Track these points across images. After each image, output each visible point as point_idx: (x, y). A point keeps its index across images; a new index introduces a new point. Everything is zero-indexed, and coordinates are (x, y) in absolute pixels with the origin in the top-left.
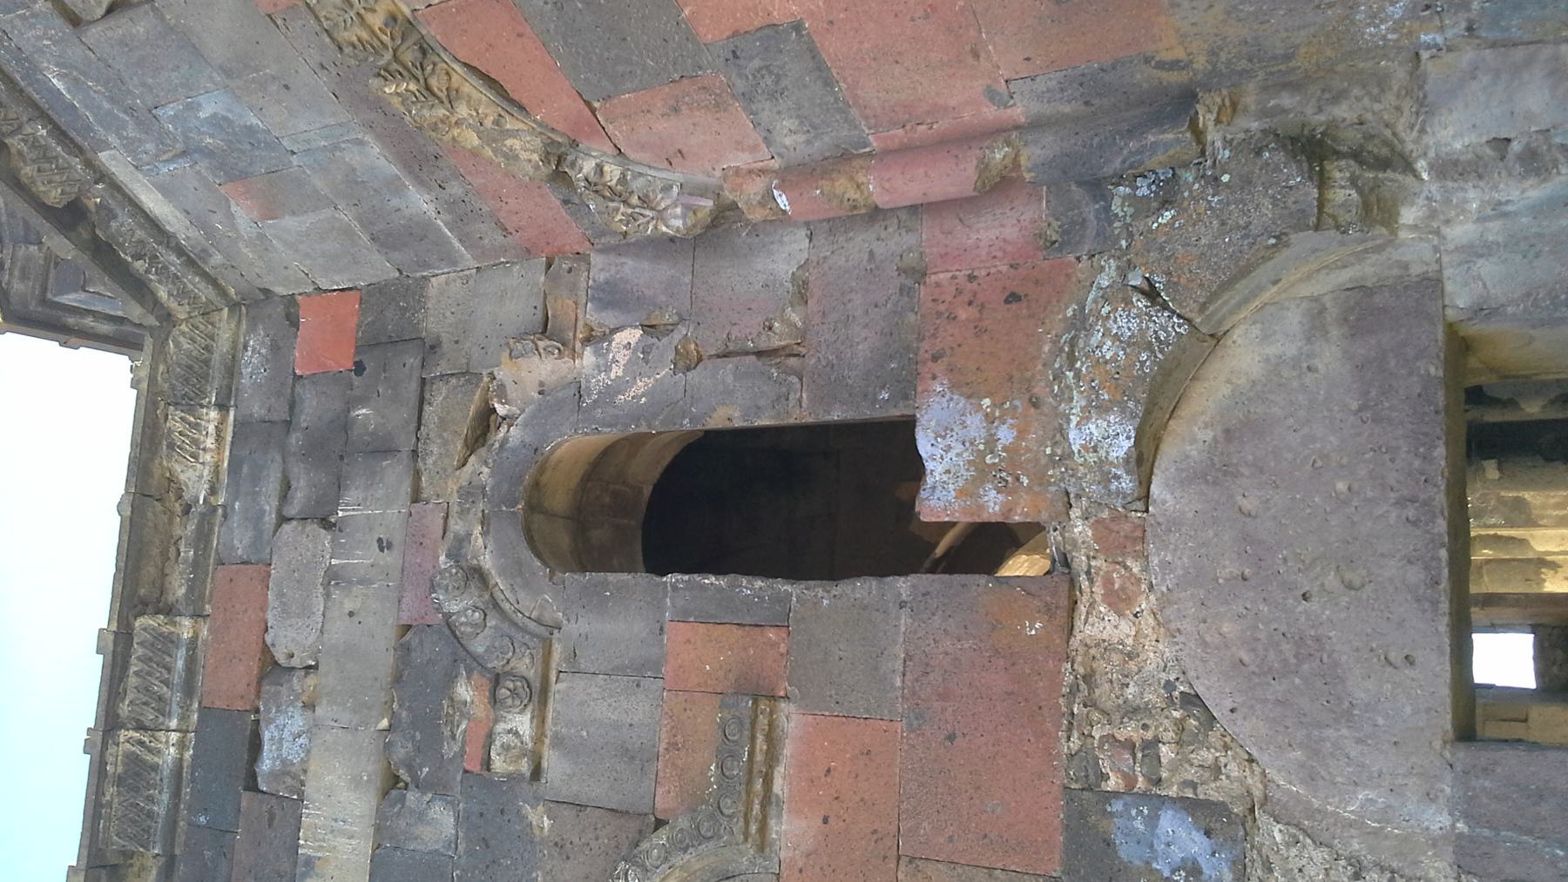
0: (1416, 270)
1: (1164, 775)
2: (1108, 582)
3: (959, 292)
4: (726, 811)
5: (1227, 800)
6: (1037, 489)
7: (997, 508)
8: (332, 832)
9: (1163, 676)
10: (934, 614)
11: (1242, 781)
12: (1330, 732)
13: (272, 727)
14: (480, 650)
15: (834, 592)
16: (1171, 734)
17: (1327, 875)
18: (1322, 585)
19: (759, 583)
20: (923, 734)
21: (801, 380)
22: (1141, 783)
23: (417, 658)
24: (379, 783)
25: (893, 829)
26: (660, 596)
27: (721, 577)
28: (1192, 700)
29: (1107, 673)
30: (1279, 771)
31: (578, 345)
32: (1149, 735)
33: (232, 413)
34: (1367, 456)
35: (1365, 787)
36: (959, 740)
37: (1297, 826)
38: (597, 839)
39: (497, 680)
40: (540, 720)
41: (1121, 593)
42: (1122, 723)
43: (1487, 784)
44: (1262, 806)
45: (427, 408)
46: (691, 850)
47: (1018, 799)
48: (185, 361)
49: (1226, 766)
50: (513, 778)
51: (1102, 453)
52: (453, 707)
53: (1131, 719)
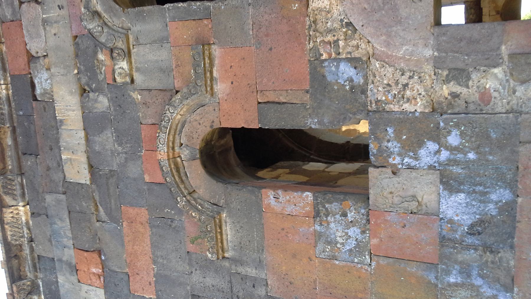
1: (341, 51)
4: (199, 85)
5: (361, 56)
8: (67, 110)
10: (261, 7)
11: (366, 49)
12: (394, 29)
13: (37, 78)
14: (104, 41)
15: (225, 3)
16: (343, 37)
17: (393, 75)
19: (198, 3)
20: (261, 50)
22: (334, 55)
23: (82, 47)
24: (79, 92)
25: (254, 82)
26: (164, 13)
27: (185, 3)
29: (321, 19)
30: (378, 44)
32: (335, 38)
35: (406, 45)
36: (273, 50)
37: (384, 61)
38: (157, 100)
39: (112, 51)
40: (130, 63)
42: (326, 35)
43: (444, 38)
44: (372, 56)
46: (189, 98)
47: (294, 66)
49: (360, 45)
50: (125, 84)
52: (98, 62)
53: (329, 34)
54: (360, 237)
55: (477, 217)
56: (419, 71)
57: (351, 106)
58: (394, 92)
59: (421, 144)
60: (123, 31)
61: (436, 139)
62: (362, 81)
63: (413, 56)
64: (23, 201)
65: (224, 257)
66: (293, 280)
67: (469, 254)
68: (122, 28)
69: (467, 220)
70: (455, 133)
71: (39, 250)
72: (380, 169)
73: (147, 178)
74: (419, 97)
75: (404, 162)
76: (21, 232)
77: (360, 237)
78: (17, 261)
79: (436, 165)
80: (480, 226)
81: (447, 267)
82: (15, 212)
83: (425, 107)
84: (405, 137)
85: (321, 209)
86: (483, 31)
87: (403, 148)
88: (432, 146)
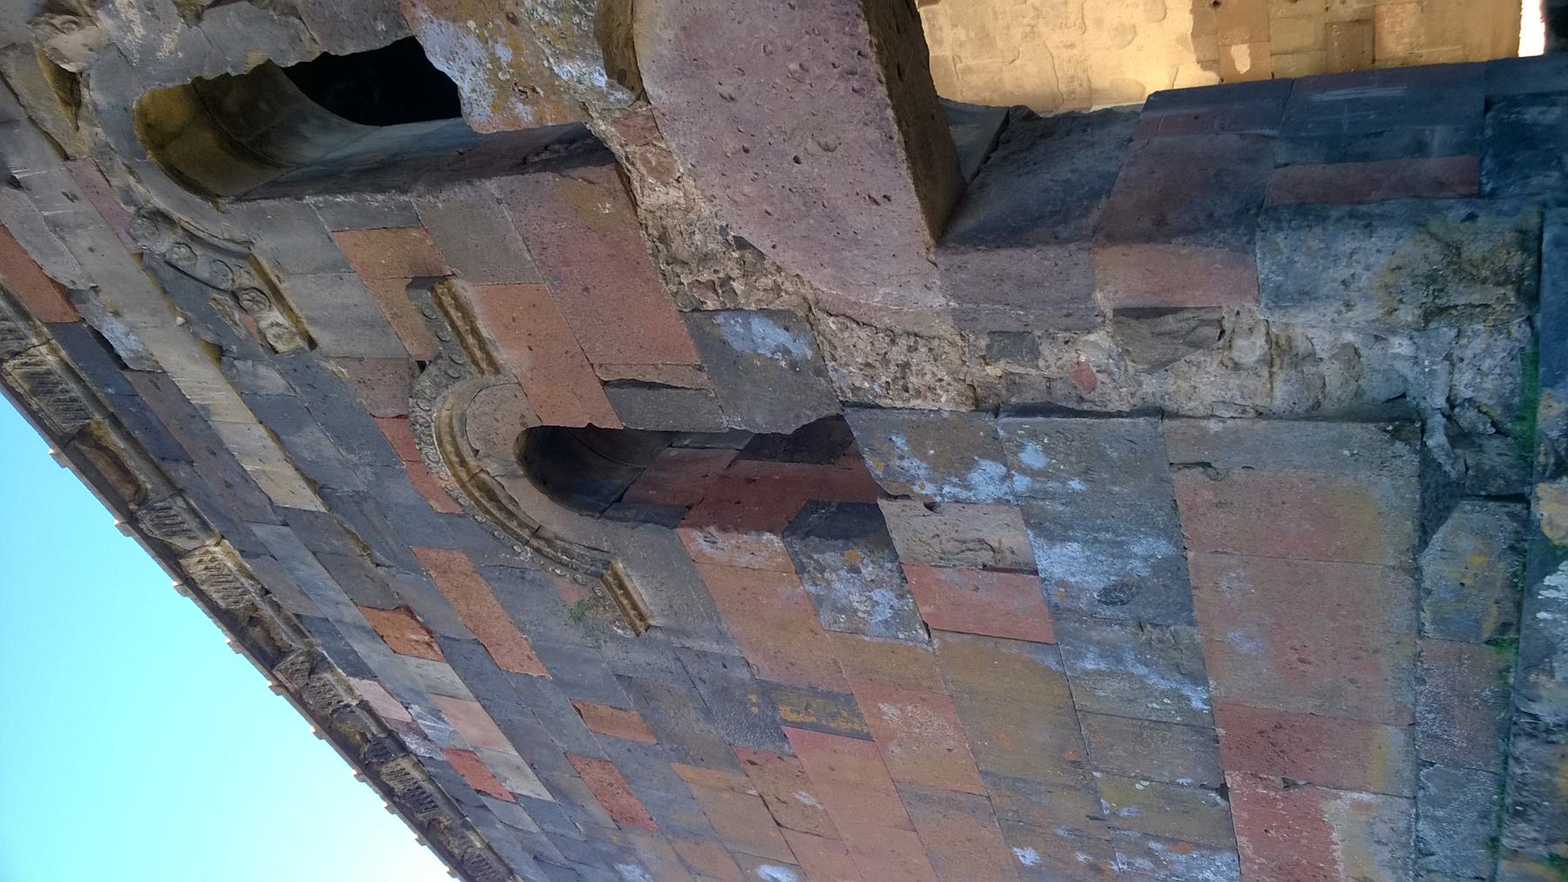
2: (646, 162)
6: (554, 98)
7: (530, 118)
9: (716, 221)
12: (846, 254)
16: (736, 271)
18: (806, 149)
19: (380, 197)
21: (301, 19)
28: (741, 244)
30: (820, 283)
34: (805, 39)
35: (882, 286)
40: (287, 310)
41: (660, 168)
43: (963, 276)
44: (817, 303)
50: (297, 352)
51: (587, 83)
55: (1112, 578)
56: (925, 333)
57: (803, 397)
58: (884, 379)
59: (970, 465)
61: (998, 456)
62: (809, 354)
63: (903, 305)
64: (211, 537)
66: (793, 661)
67: (1112, 631)
68: (233, 241)
69: (1094, 582)
70: (1031, 447)
72: (900, 502)
74: (942, 387)
75: (944, 492)
76: (238, 585)
77: (895, 602)
78: (258, 629)
79: (1010, 498)
80: (1121, 591)
81: (1075, 648)
84: (932, 452)
85: (805, 560)
86: (1046, 263)
87: (934, 468)
88: (994, 469)
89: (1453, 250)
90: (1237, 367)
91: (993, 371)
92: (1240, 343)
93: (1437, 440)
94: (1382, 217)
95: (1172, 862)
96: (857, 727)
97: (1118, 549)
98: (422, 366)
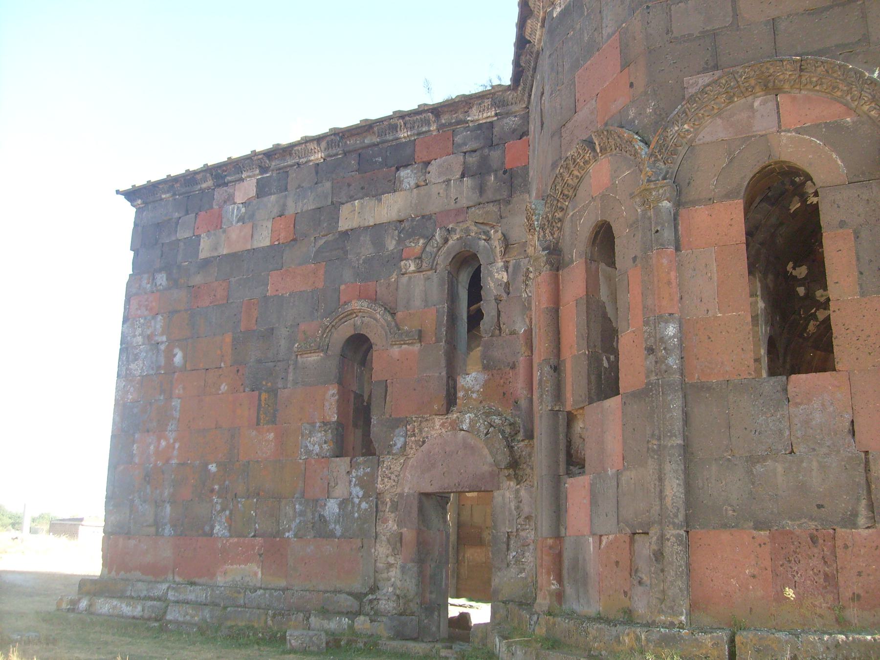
0: (501, 485)
3: (507, 379)
14: (427, 249)
28: (424, 442)
31: (504, 260)
33: (495, 118)
40: (414, 272)
44: (409, 458)
45: (492, 204)
48: (505, 99)
54: (314, 452)
59: (362, 488)
60: (434, 267)
61: (364, 496)
62: (394, 452)
64: (325, 157)
65: (297, 355)
69: (326, 513)
71: (292, 175)
73: (343, 287)
77: (314, 452)
82: (316, 150)
83: (379, 489)
88: (361, 494)
89: (411, 601)
90: (387, 557)
91: (388, 500)
92: (393, 558)
93: (370, 597)
94: (419, 588)
95: (221, 516)
96: (262, 421)
97: (337, 522)
98: (393, 314)
